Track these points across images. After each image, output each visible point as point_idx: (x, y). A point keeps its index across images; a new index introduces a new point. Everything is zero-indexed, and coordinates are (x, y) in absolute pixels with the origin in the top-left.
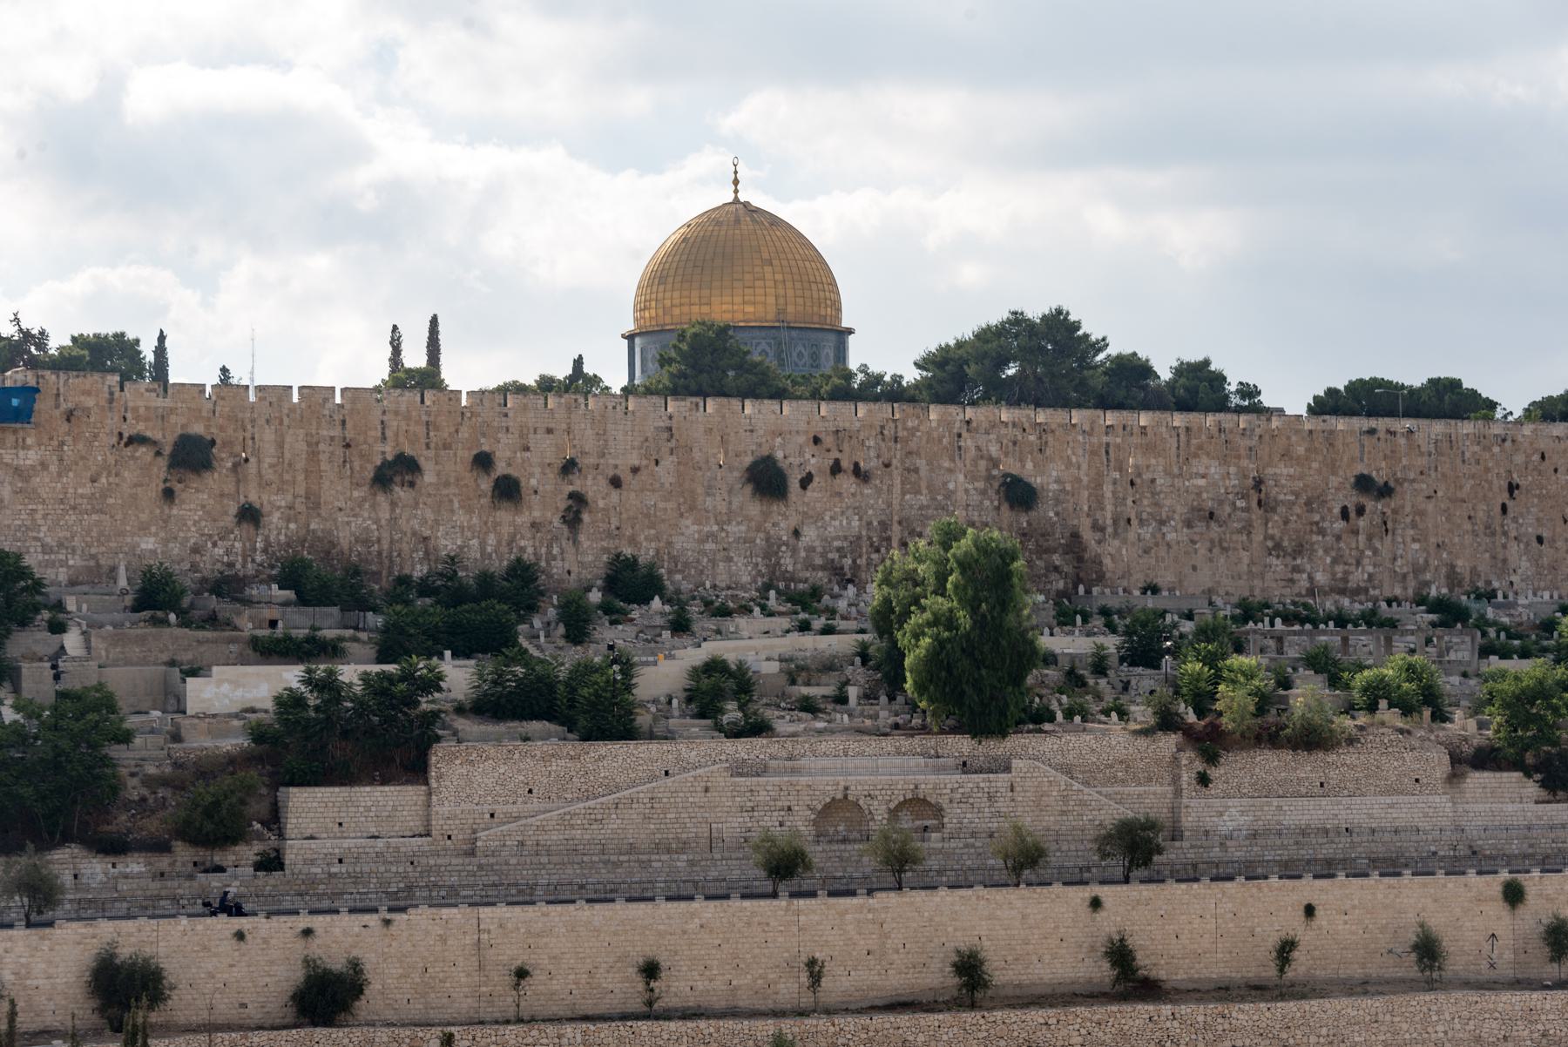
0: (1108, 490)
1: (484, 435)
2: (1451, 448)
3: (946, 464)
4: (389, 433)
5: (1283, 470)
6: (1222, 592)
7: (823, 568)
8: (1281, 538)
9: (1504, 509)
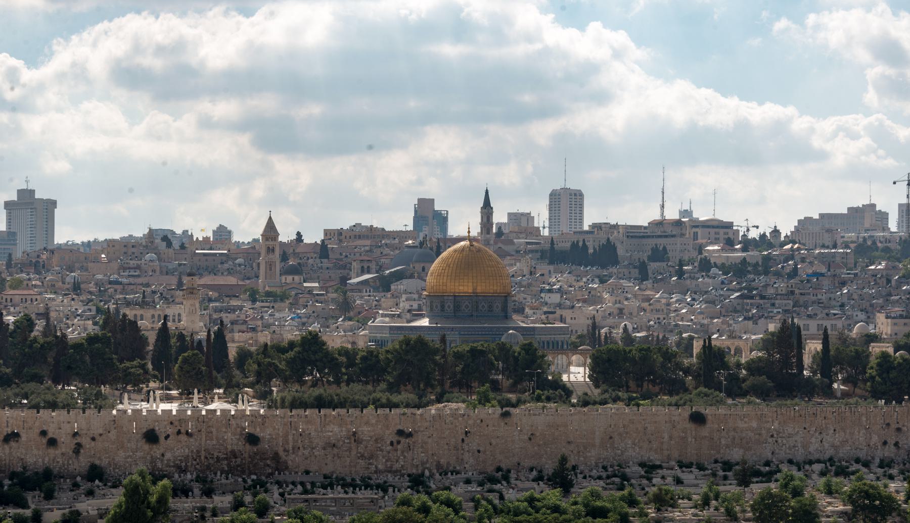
0: (290, 438)
1: (44, 424)
2: (440, 419)
3: (224, 430)
4: (9, 425)
5: (365, 428)
7: (173, 466)
8: (364, 453)
9: (463, 440)
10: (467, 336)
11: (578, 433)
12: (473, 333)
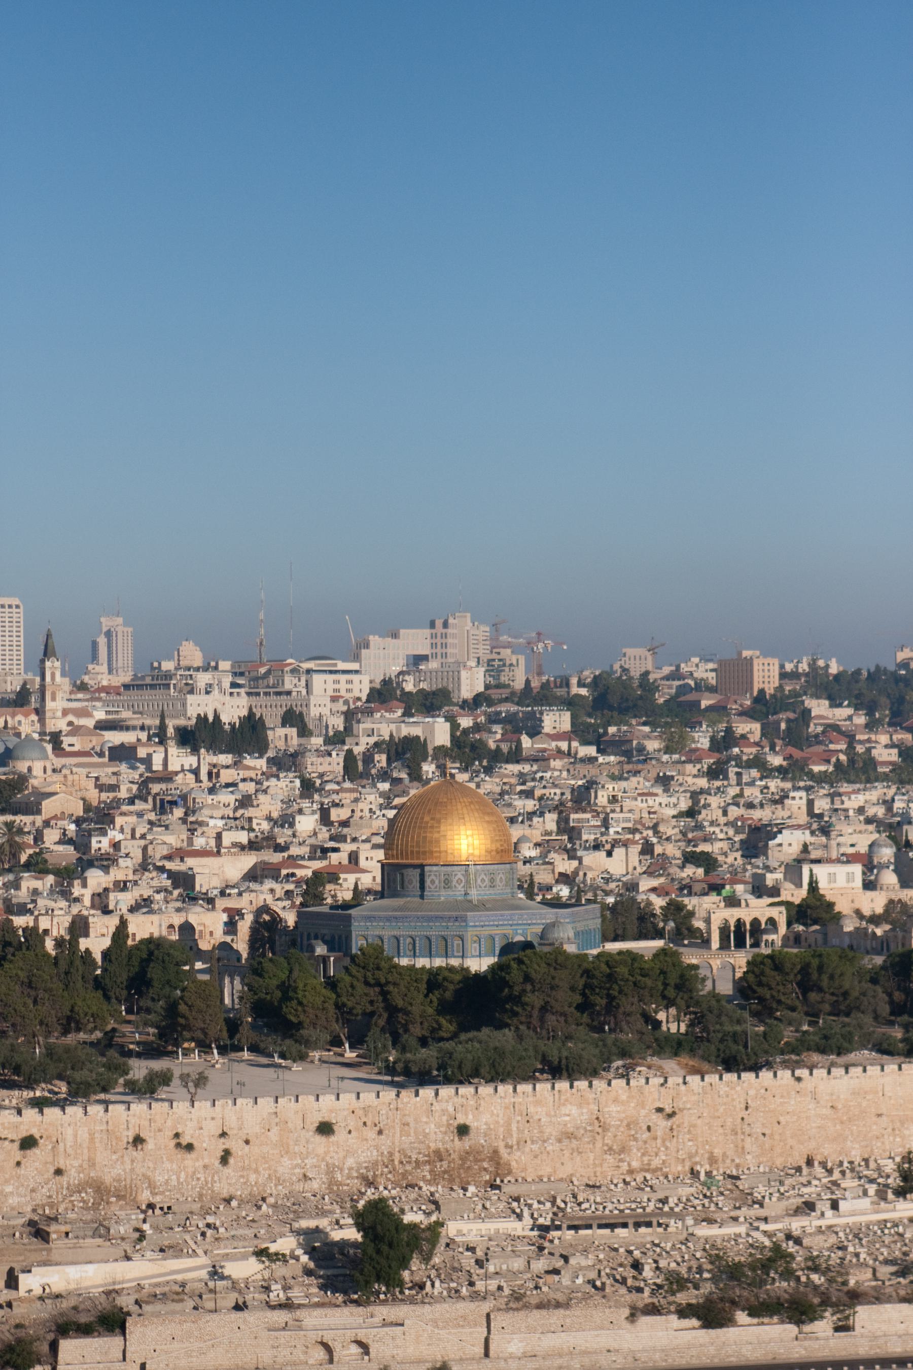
0: (514, 1127)
3: (425, 1119)
4: (130, 1126)
5: (614, 1108)
6: (578, 1175)
7: (357, 1177)
9: (743, 1119)
10: (479, 929)
11: (892, 1102)
12: (487, 923)
